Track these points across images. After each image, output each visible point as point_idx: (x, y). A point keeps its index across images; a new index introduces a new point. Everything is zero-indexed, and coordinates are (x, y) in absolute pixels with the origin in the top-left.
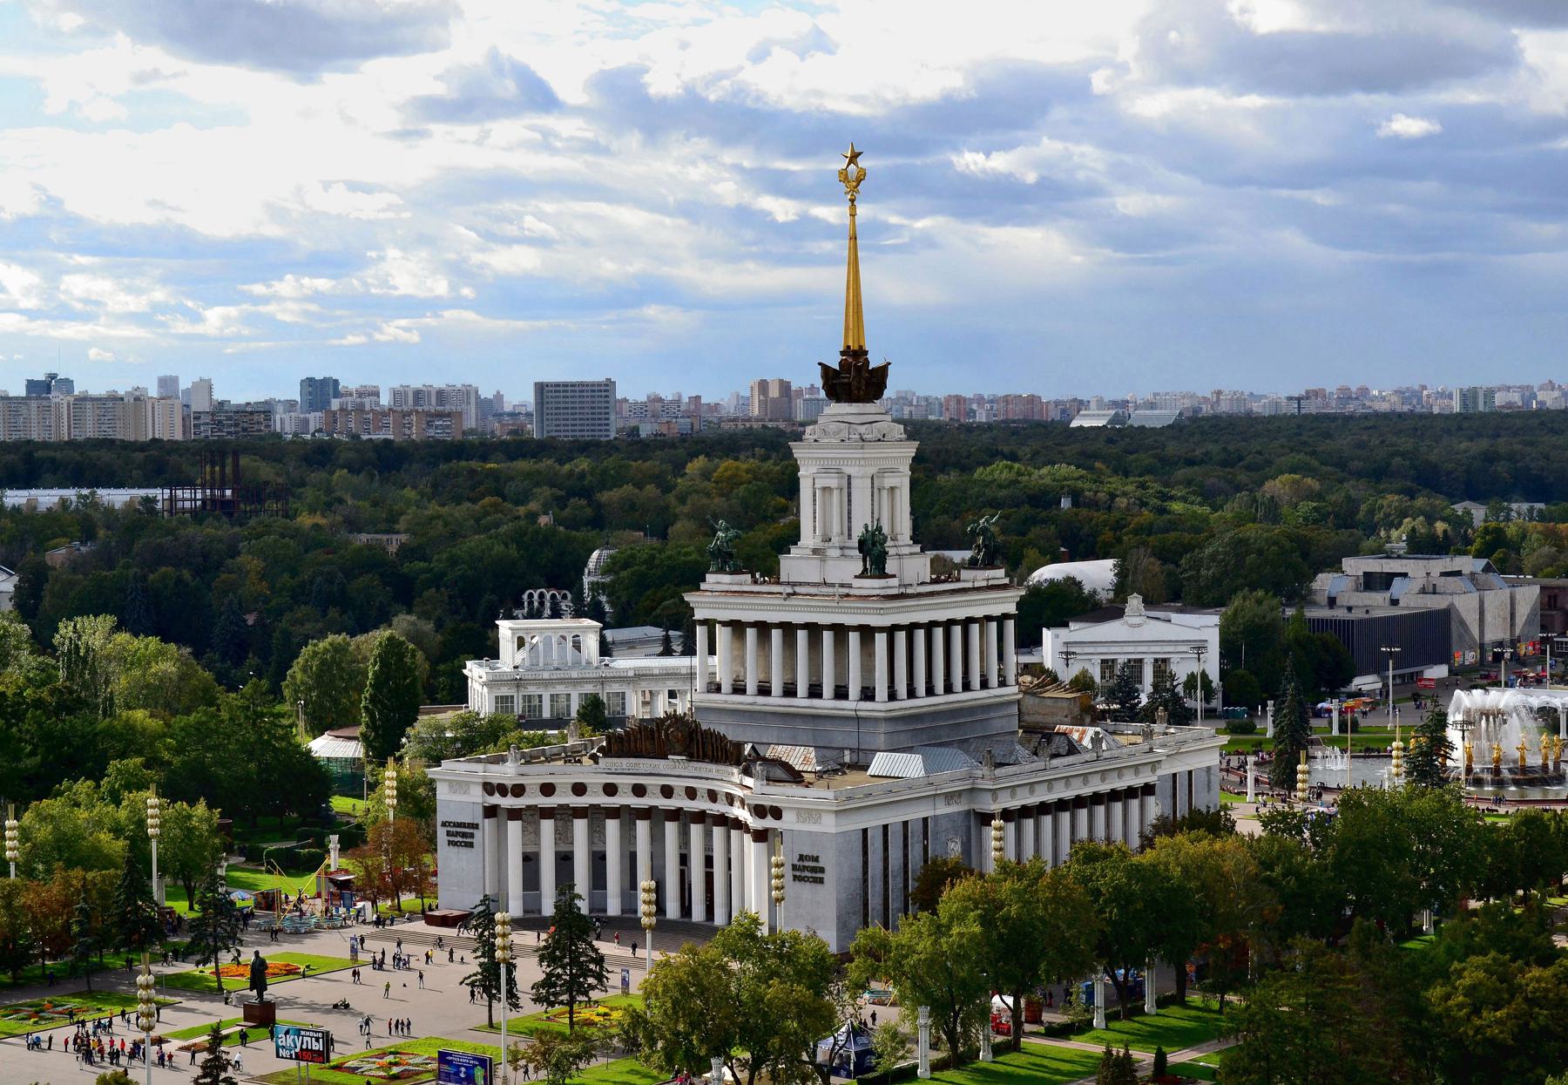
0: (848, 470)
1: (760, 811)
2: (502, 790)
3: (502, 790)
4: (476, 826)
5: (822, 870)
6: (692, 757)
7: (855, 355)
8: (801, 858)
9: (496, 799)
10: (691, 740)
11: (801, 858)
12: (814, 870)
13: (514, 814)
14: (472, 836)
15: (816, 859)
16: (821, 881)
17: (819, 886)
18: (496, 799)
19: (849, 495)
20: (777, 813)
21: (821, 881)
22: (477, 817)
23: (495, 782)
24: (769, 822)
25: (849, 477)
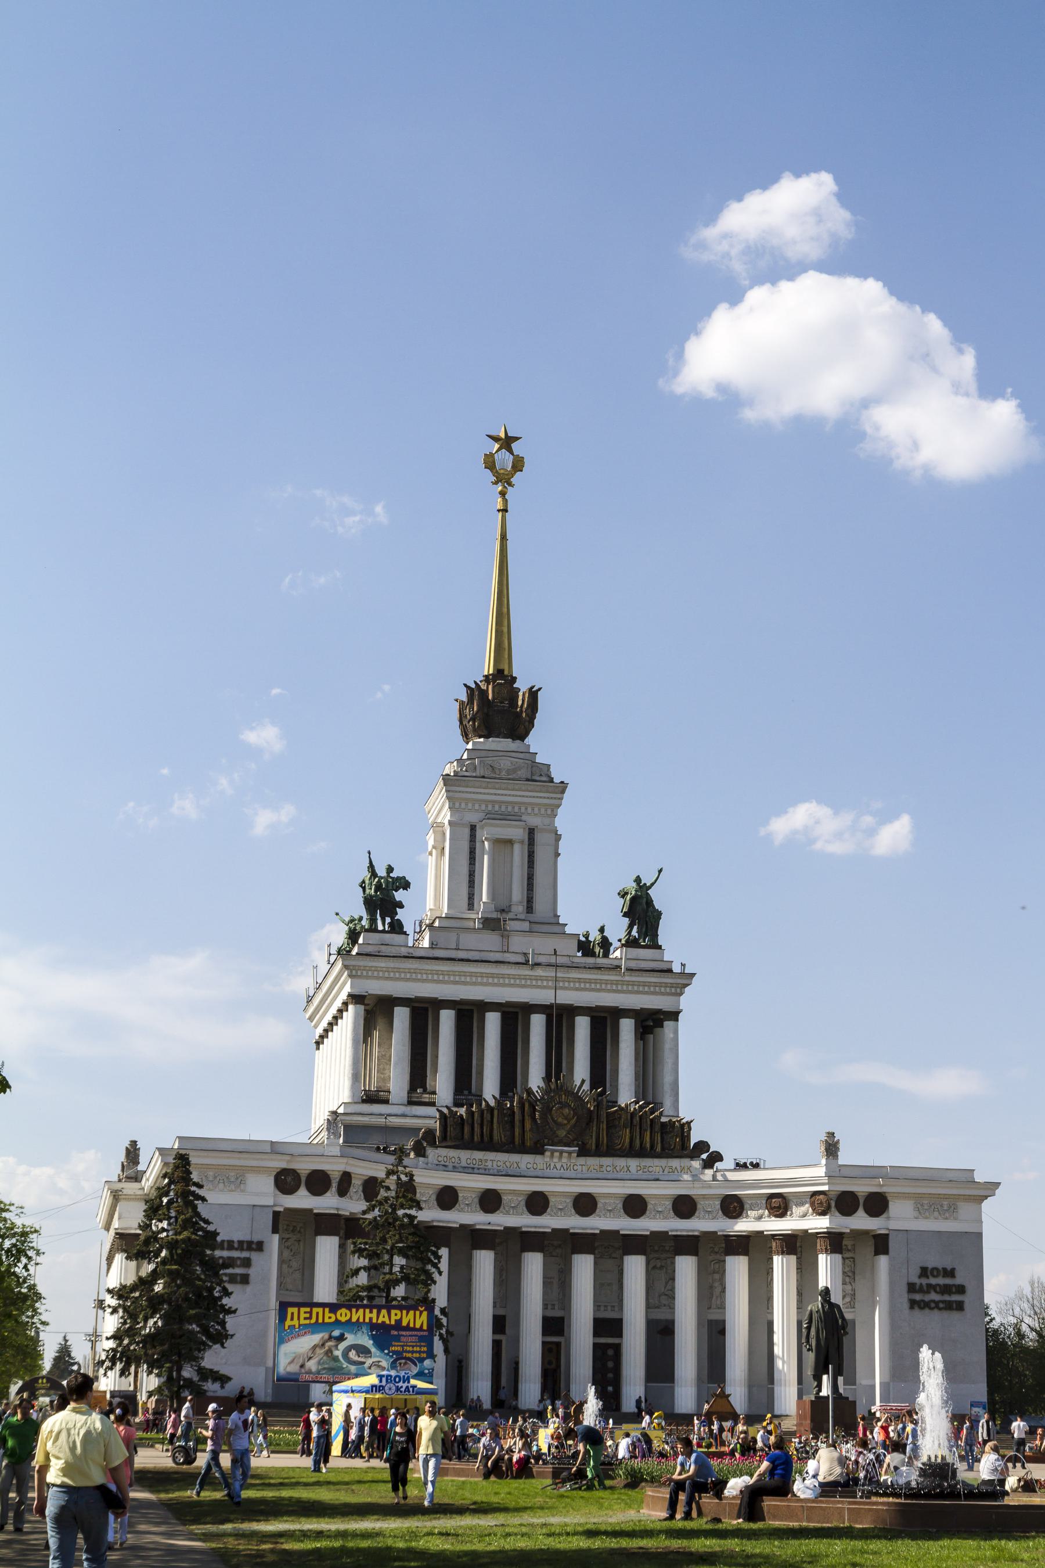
2: (318, 1182)
3: (318, 1182)
4: (259, 1246)
5: (961, 1289)
6: (583, 1152)
8: (924, 1272)
9: (302, 1200)
10: (590, 1120)
11: (924, 1272)
12: (946, 1289)
13: (326, 1223)
14: (247, 1263)
15: (950, 1273)
16: (960, 1306)
17: (955, 1315)
18: (302, 1200)
19: (531, 855)
20: (877, 1204)
21: (960, 1306)
22: (263, 1230)
23: (304, 1167)
24: (860, 1221)
25: (531, 832)
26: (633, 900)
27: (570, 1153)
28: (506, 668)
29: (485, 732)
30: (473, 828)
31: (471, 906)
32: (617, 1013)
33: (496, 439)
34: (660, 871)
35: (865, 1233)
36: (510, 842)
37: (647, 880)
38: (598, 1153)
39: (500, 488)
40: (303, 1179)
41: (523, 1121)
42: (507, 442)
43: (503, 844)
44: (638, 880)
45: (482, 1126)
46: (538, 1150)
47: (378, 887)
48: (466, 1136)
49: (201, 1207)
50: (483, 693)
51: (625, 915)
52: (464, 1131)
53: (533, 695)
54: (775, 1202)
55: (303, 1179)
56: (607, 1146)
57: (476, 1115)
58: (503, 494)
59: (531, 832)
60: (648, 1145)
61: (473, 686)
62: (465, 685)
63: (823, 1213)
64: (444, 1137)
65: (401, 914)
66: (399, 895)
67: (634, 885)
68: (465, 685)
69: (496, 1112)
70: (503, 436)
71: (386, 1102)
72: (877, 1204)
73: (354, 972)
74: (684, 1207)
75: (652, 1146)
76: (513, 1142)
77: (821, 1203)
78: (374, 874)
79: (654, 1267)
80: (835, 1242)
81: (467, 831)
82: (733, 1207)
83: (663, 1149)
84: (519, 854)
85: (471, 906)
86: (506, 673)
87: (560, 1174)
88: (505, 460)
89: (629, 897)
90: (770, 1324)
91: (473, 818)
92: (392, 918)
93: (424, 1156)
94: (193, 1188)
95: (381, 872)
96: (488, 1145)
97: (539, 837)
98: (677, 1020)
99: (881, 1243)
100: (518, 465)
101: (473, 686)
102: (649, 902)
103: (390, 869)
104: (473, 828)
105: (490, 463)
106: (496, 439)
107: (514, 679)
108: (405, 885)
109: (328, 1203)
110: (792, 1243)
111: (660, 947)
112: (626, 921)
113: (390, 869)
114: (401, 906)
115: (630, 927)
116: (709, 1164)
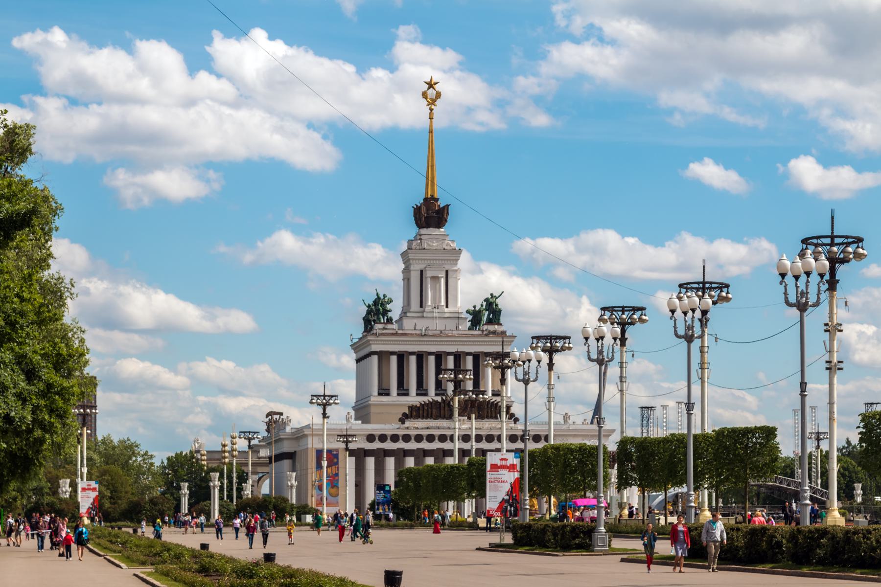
7: (430, 200)
25: (447, 272)
37: (496, 294)
42: (431, 85)
43: (435, 279)
44: (492, 295)
58: (431, 110)
59: (447, 272)
71: (388, 394)
78: (379, 298)
84: (443, 281)
85: (421, 306)
88: (431, 93)
91: (422, 267)
97: (450, 273)
100: (438, 95)
103: (385, 296)
104: (422, 272)
105: (424, 95)
113: (385, 296)
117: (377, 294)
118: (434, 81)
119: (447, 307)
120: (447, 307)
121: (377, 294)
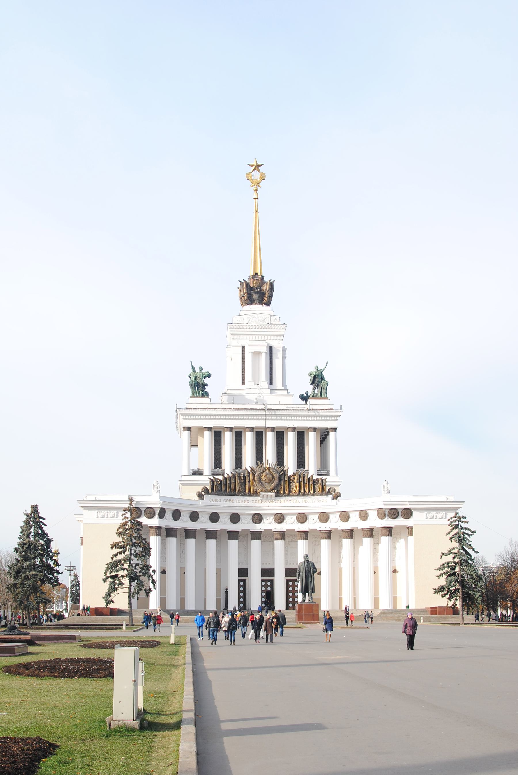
0: (271, 343)
1: (394, 513)
2: (150, 513)
3: (150, 513)
6: (278, 494)
20: (408, 513)
24: (400, 521)
25: (271, 348)
26: (315, 377)
27: (271, 496)
28: (258, 271)
29: (250, 302)
30: (244, 347)
31: (244, 383)
32: (308, 429)
33: (252, 166)
34: (327, 363)
35: (403, 526)
36: (260, 353)
38: (284, 495)
39: (255, 189)
40: (143, 512)
41: (249, 482)
43: (256, 354)
45: (230, 484)
46: (256, 494)
47: (196, 377)
48: (223, 489)
49: (45, 528)
50: (247, 284)
51: (312, 384)
52: (221, 487)
53: (272, 284)
54: (363, 514)
55: (143, 512)
56: (290, 491)
57: (227, 480)
60: (307, 491)
61: (243, 281)
62: (240, 282)
63: (382, 518)
64: (212, 491)
65: (207, 389)
66: (206, 381)
67: (315, 370)
68: (240, 282)
69: (237, 478)
70: (255, 164)
71: (202, 474)
72: (408, 513)
73: (185, 417)
74: (324, 517)
75: (309, 491)
76: (245, 491)
77: (381, 514)
78: (194, 371)
79: (315, 545)
80: (389, 531)
81: (241, 349)
82: (345, 516)
83: (314, 491)
85: (244, 383)
86: (259, 274)
87: (267, 504)
88: (256, 175)
89: (313, 376)
90: (340, 569)
91: (244, 343)
92: (203, 391)
93: (203, 499)
94: (41, 520)
95: (197, 370)
96: (233, 493)
98: (336, 432)
99: (410, 530)
101: (243, 281)
102: (322, 378)
103: (201, 369)
104: (244, 347)
105: (248, 177)
106: (252, 166)
107: (263, 277)
108: (209, 376)
109: (155, 522)
110: (370, 532)
111: (327, 398)
112: (312, 387)
113: (201, 369)
114: (207, 386)
115: (314, 389)
116: (336, 497)
117: (193, 368)
118: (259, 163)
119: (271, 383)
120: (271, 383)
121: (193, 368)
